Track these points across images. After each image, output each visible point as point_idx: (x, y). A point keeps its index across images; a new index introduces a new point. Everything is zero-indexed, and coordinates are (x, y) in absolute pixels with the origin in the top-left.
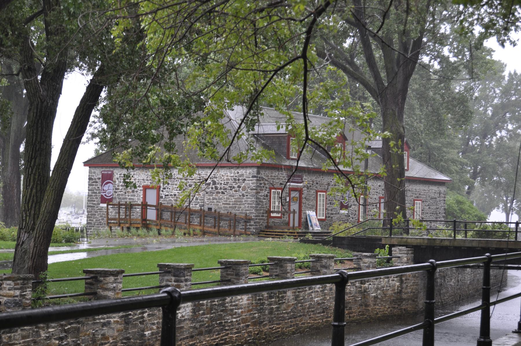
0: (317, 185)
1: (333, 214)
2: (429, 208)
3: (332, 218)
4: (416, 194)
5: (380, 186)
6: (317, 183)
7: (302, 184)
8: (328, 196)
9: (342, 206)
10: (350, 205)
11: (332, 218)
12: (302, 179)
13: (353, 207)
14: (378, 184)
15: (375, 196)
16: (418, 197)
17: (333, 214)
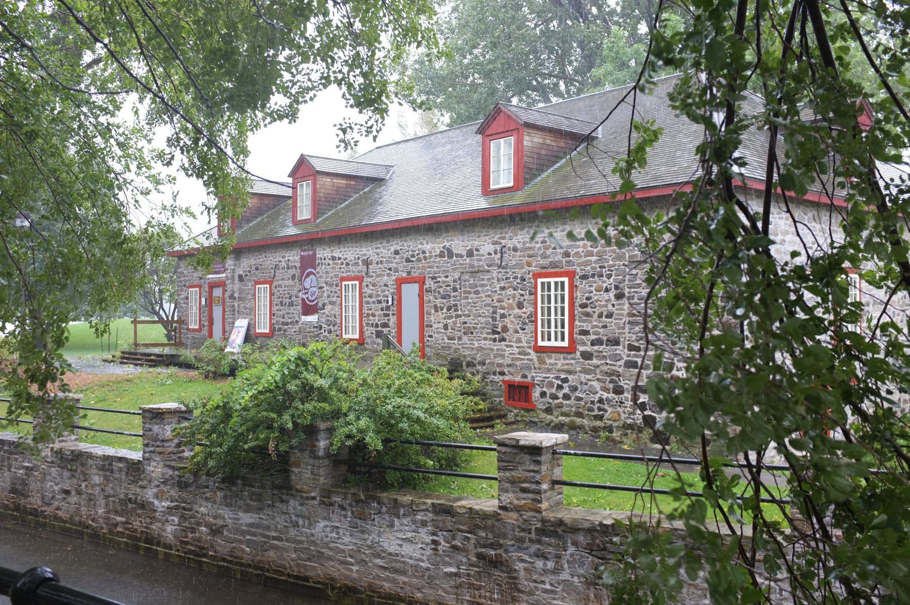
0: (257, 272)
1: (287, 324)
2: (619, 296)
3: (285, 331)
4: (545, 256)
5: (396, 252)
6: (257, 269)
7: (224, 275)
8: (275, 291)
9: (308, 309)
10: (320, 305)
11: (285, 331)
12: (224, 267)
13: (328, 307)
14: (392, 249)
15: (386, 278)
16: (554, 265)
17: (287, 324)
